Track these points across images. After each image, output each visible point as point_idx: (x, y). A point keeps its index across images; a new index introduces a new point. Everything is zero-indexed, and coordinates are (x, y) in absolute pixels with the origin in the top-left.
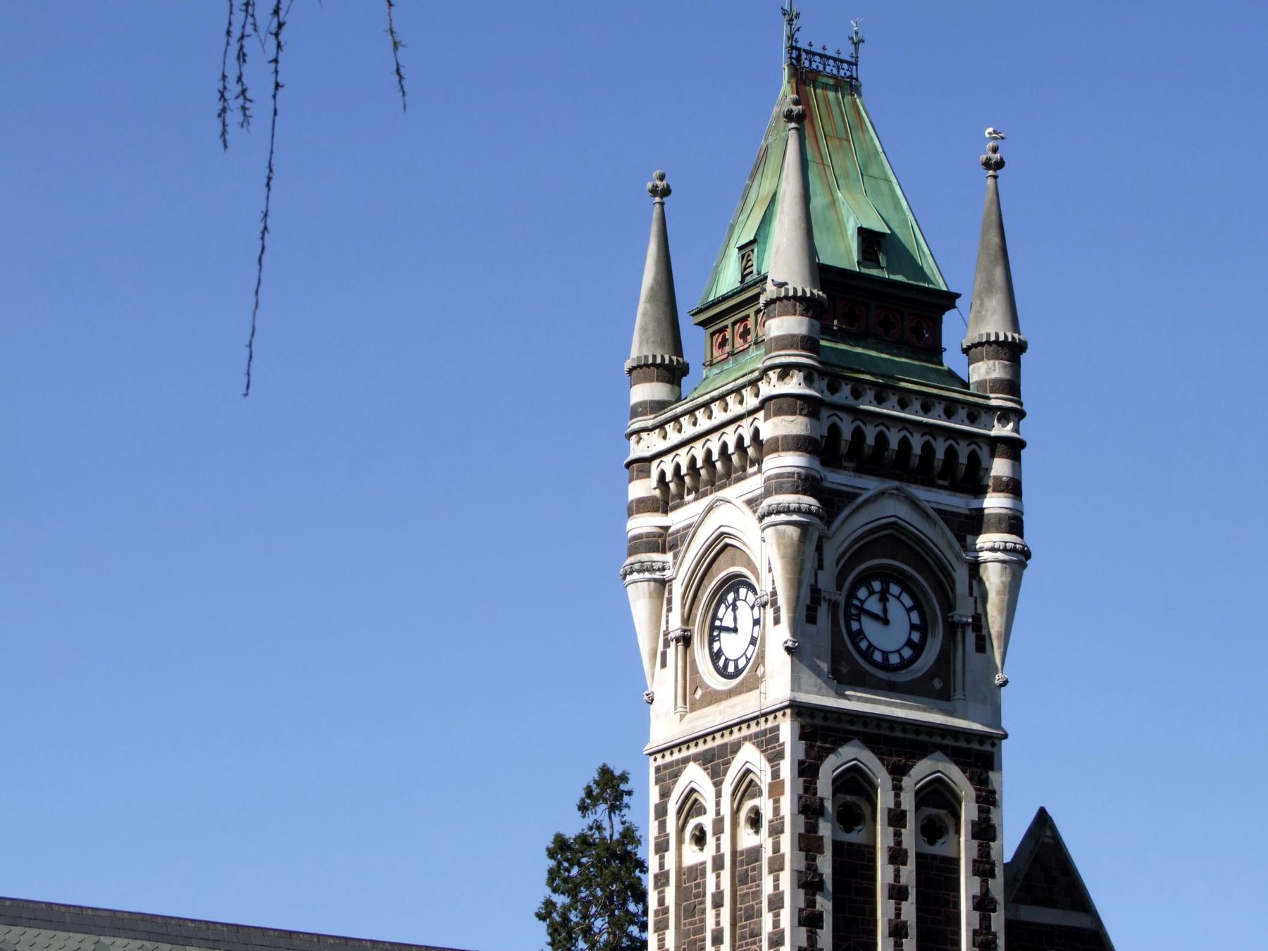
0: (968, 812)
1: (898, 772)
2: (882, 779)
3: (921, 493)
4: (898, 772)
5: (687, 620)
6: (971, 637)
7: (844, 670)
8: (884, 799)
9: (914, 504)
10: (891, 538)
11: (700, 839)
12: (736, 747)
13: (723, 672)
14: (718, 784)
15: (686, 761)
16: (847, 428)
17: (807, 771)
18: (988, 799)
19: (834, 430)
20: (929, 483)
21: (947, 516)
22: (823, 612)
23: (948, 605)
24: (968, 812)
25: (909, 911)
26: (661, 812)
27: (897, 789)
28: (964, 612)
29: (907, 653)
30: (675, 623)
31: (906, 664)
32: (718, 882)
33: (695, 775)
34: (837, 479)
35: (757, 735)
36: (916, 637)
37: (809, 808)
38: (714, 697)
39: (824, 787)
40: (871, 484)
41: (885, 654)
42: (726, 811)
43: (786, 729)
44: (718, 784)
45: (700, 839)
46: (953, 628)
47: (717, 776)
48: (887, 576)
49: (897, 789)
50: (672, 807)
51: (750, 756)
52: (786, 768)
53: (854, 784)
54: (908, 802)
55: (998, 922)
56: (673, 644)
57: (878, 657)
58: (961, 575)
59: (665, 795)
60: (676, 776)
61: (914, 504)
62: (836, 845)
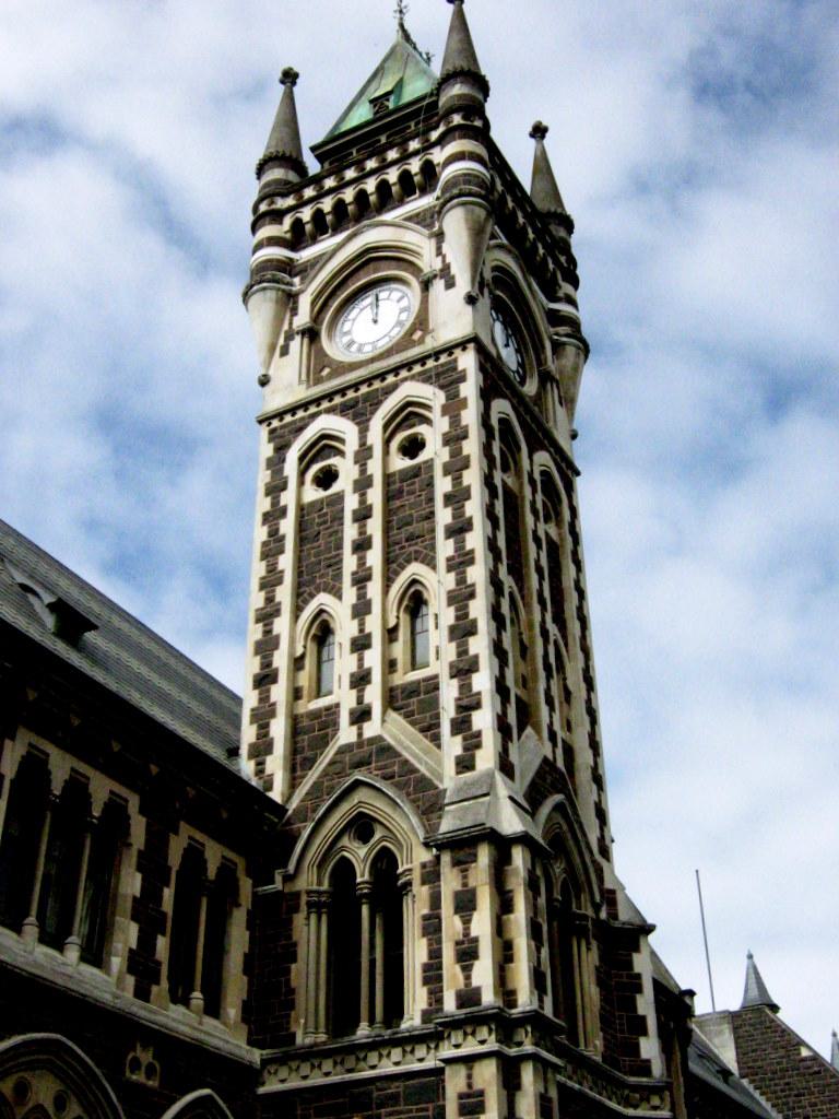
15: (314, 416)
35: (420, 374)
43: (467, 361)
56: (298, 338)
58: (548, 345)
59: (281, 450)
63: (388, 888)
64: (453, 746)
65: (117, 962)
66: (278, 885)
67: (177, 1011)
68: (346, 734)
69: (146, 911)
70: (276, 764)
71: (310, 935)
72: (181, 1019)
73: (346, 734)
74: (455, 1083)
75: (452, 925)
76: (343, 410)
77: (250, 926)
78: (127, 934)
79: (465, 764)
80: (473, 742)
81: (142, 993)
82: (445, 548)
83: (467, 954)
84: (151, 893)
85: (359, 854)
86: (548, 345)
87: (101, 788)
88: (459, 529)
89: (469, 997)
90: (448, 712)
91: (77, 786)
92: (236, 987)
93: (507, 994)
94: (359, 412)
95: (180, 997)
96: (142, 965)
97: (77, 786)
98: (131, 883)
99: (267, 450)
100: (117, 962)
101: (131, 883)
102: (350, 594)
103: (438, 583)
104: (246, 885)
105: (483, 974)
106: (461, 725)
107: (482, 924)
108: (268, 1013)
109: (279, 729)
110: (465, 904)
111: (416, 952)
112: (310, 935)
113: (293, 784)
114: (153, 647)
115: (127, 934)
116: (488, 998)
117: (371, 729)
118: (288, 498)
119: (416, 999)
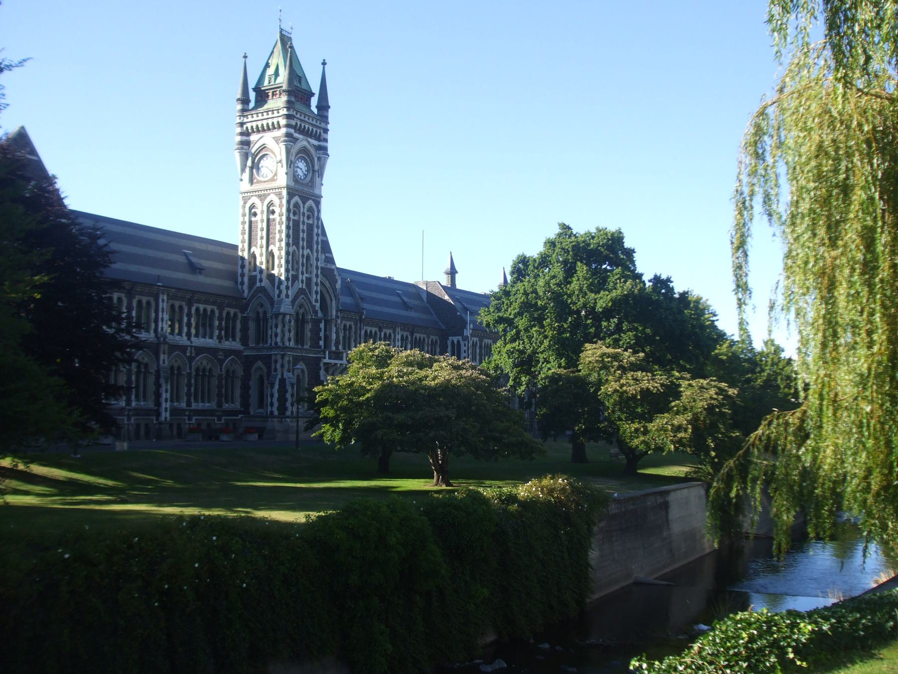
1: (304, 203)
4: (304, 203)
8: (302, 210)
9: (309, 142)
11: (255, 214)
17: (288, 202)
18: (319, 211)
23: (313, 166)
26: (244, 207)
28: (316, 168)
33: (255, 200)
34: (296, 135)
37: (288, 210)
40: (301, 136)
46: (314, 171)
47: (262, 201)
48: (303, 158)
52: (284, 201)
53: (296, 205)
58: (316, 159)
59: (245, 203)
61: (309, 142)
63: (266, 320)
64: (277, 292)
65: (215, 338)
67: (227, 343)
68: (258, 284)
69: (220, 328)
70: (246, 287)
71: (252, 325)
72: (227, 344)
73: (258, 284)
74: (273, 358)
75: (274, 329)
76: (259, 196)
78: (217, 332)
79: (279, 296)
80: (280, 292)
81: (220, 342)
82: (277, 244)
83: (276, 335)
84: (220, 324)
85: (261, 310)
86: (316, 159)
87: (209, 308)
88: (281, 240)
89: (276, 343)
90: (276, 284)
91: (205, 310)
92: (238, 335)
93: (283, 343)
94: (262, 198)
95: (227, 340)
96: (220, 338)
97: (205, 310)
98: (217, 323)
99: (242, 203)
100: (215, 338)
101: (217, 323)
102: (259, 249)
103: (276, 253)
104: (239, 315)
105: (279, 339)
106: (279, 288)
107: (279, 330)
108: (244, 341)
109: (246, 279)
110: (276, 326)
111: (269, 332)
112: (252, 325)
113: (249, 291)
114: (218, 249)
115: (217, 332)
116: (280, 344)
117: (263, 284)
119: (269, 341)
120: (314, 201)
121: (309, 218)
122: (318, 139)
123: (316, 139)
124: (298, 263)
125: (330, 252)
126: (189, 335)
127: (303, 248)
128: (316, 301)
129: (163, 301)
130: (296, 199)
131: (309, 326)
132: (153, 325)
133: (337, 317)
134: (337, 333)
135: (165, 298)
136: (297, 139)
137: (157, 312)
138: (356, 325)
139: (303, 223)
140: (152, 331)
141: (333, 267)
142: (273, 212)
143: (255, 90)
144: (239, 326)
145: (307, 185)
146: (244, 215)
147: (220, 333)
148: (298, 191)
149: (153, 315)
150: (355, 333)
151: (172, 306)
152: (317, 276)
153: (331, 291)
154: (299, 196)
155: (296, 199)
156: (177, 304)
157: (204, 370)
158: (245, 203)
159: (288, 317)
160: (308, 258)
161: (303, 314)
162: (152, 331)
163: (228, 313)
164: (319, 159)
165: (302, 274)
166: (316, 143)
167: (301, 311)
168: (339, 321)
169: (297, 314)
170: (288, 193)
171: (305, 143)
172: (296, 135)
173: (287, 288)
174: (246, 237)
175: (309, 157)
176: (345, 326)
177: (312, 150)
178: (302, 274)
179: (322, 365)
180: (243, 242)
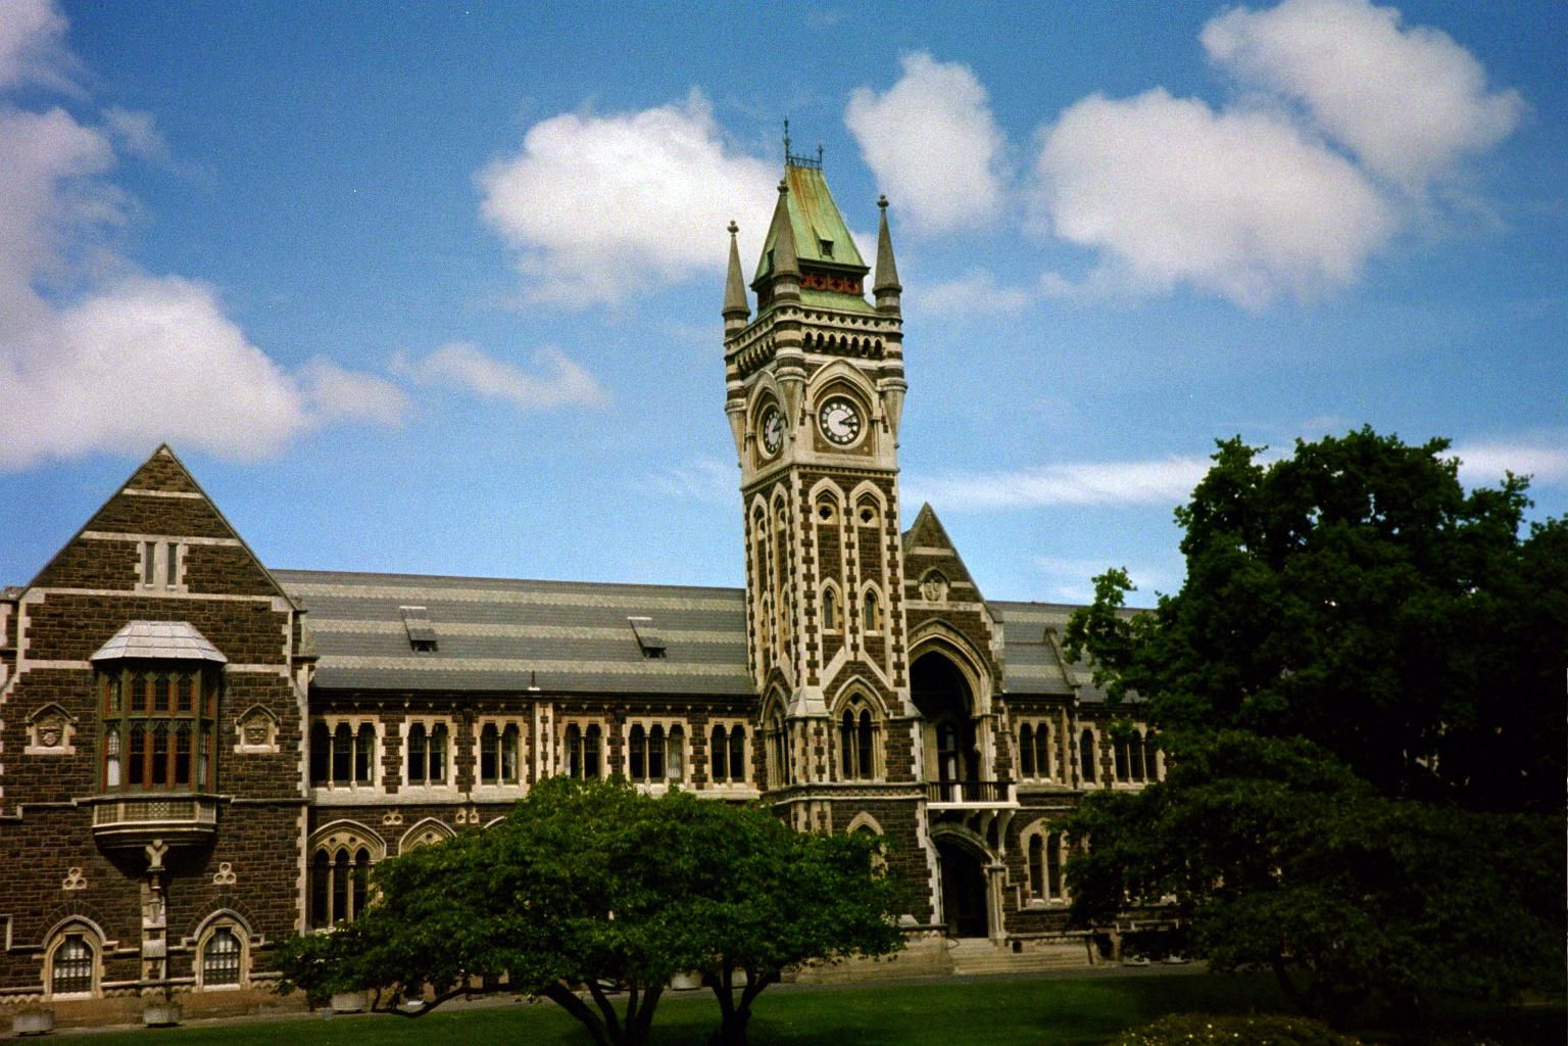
0: (884, 506)
1: (847, 490)
2: (840, 494)
3: (850, 360)
4: (847, 490)
5: (755, 427)
6: (881, 426)
7: (820, 446)
8: (842, 504)
10: (841, 383)
11: (763, 528)
12: (774, 485)
13: (769, 451)
14: (768, 503)
15: (755, 493)
16: (815, 334)
17: (804, 493)
18: (891, 500)
19: (809, 336)
20: (858, 356)
21: (868, 372)
22: (808, 419)
23: (870, 412)
24: (884, 506)
25: (856, 553)
27: (847, 498)
28: (877, 414)
29: (851, 436)
30: (749, 430)
31: (850, 441)
32: (772, 546)
33: (759, 499)
34: (810, 358)
36: (855, 428)
38: (766, 463)
39: (812, 500)
40: (829, 359)
41: (840, 437)
42: (772, 514)
44: (768, 503)
45: (763, 528)
46: (872, 423)
48: (840, 400)
49: (847, 498)
50: (752, 514)
51: (779, 489)
54: (853, 504)
55: (900, 556)
57: (837, 439)
58: (875, 397)
59: (748, 509)
60: (752, 501)
61: (851, 366)
62: (820, 528)
66: (759, 728)
68: (772, 666)
77: (753, 744)
86: (875, 397)
87: (667, 723)
91: (657, 729)
92: (749, 769)
94: (766, 493)
104: (749, 731)
108: (760, 779)
118: (752, 537)
120: (876, 481)
121: (866, 516)
122: (877, 353)
123: (871, 357)
124: (841, 610)
125: (964, 576)
126: (1075, 778)
127: (852, 579)
128: (899, 683)
129: (544, 720)
130: (825, 483)
131: (880, 739)
132: (525, 769)
133: (996, 710)
134: (1000, 744)
135: (550, 713)
136: (810, 368)
137: (531, 742)
138: (1058, 723)
139: (849, 529)
140: (523, 781)
141: (977, 607)
142: (783, 518)
143: (754, 286)
144: (749, 750)
145: (858, 451)
146: (748, 533)
147: (699, 770)
148: (824, 467)
149: (524, 749)
150: (1059, 740)
151: (573, 729)
152: (897, 632)
153: (974, 658)
154: (831, 477)
155: (825, 483)
156: (583, 723)
157: (343, 855)
158: (748, 509)
159: (812, 725)
160: (871, 597)
161: (865, 715)
162: (523, 781)
163: (719, 730)
164: (882, 395)
165: (854, 631)
166: (874, 365)
167: (858, 708)
168: (1005, 718)
169: (848, 715)
170: (802, 476)
171: (840, 370)
172: (810, 358)
173: (813, 665)
174: (755, 573)
175: (856, 394)
176: (1026, 728)
177: (863, 382)
178: (854, 631)
179: (920, 815)
180: (750, 584)
